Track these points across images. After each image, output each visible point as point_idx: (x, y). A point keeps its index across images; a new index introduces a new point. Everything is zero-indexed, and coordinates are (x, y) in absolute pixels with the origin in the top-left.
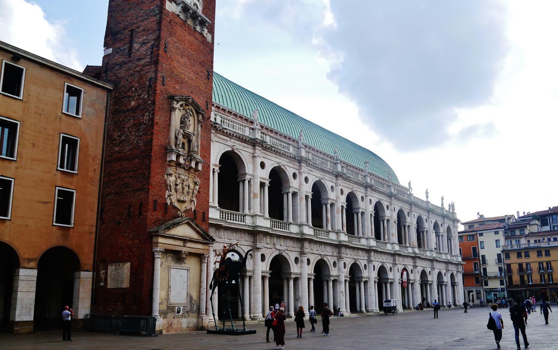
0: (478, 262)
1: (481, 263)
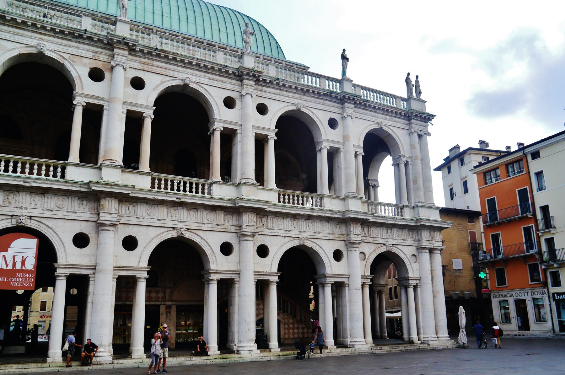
0: (533, 225)
1: (541, 225)
